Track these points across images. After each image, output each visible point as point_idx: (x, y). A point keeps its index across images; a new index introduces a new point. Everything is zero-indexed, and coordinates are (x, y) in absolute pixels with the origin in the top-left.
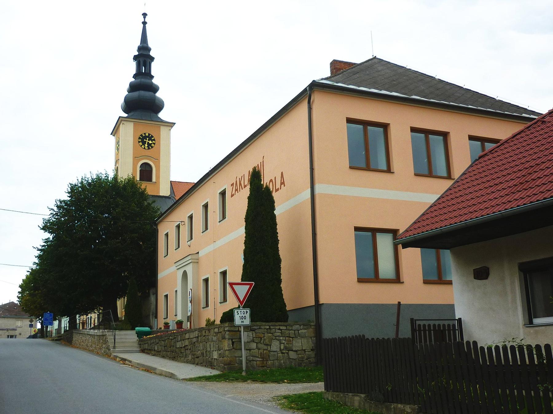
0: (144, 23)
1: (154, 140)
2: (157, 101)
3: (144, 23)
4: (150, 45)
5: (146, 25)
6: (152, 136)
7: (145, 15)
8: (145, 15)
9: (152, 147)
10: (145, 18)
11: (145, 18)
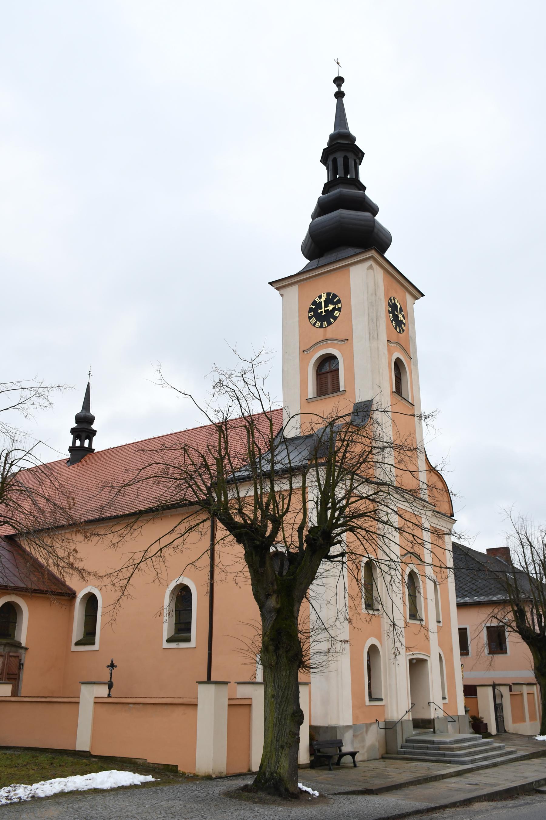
0: (339, 95)
1: (339, 302)
2: (376, 230)
3: (339, 95)
4: (353, 129)
5: (344, 99)
6: (335, 296)
7: (339, 81)
8: (339, 81)
9: (335, 318)
10: (339, 86)
11: (339, 86)
